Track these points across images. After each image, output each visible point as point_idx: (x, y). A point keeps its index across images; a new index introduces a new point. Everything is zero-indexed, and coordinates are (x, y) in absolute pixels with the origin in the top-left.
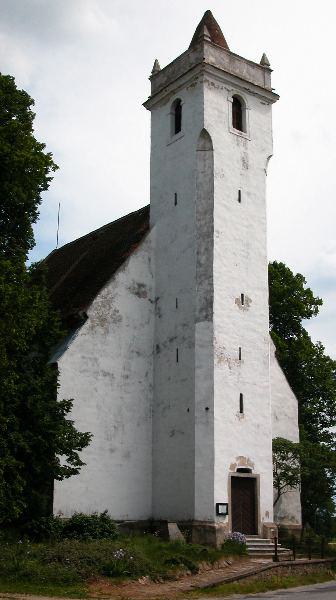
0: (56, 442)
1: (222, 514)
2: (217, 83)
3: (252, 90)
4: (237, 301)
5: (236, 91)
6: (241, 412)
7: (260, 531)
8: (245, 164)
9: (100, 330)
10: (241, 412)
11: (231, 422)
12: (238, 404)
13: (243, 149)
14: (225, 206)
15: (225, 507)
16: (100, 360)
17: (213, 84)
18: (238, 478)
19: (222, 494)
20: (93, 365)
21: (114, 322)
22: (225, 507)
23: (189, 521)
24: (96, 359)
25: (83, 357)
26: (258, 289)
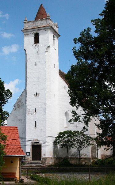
0: (90, 117)
1: (28, 155)
2: (28, 33)
3: (40, 29)
4: (35, 95)
5: (35, 32)
6: (36, 126)
7: (41, 159)
8: (38, 53)
9: (18, 109)
10: (36, 126)
11: (32, 130)
12: (37, 125)
13: (37, 49)
14: (31, 69)
15: (29, 153)
16: (18, 116)
17: (27, 34)
18: (34, 145)
19: (29, 149)
20: (16, 118)
21: (22, 106)
22: (29, 153)
23: (50, 153)
24: (17, 117)
25: (13, 117)
26: (42, 89)
